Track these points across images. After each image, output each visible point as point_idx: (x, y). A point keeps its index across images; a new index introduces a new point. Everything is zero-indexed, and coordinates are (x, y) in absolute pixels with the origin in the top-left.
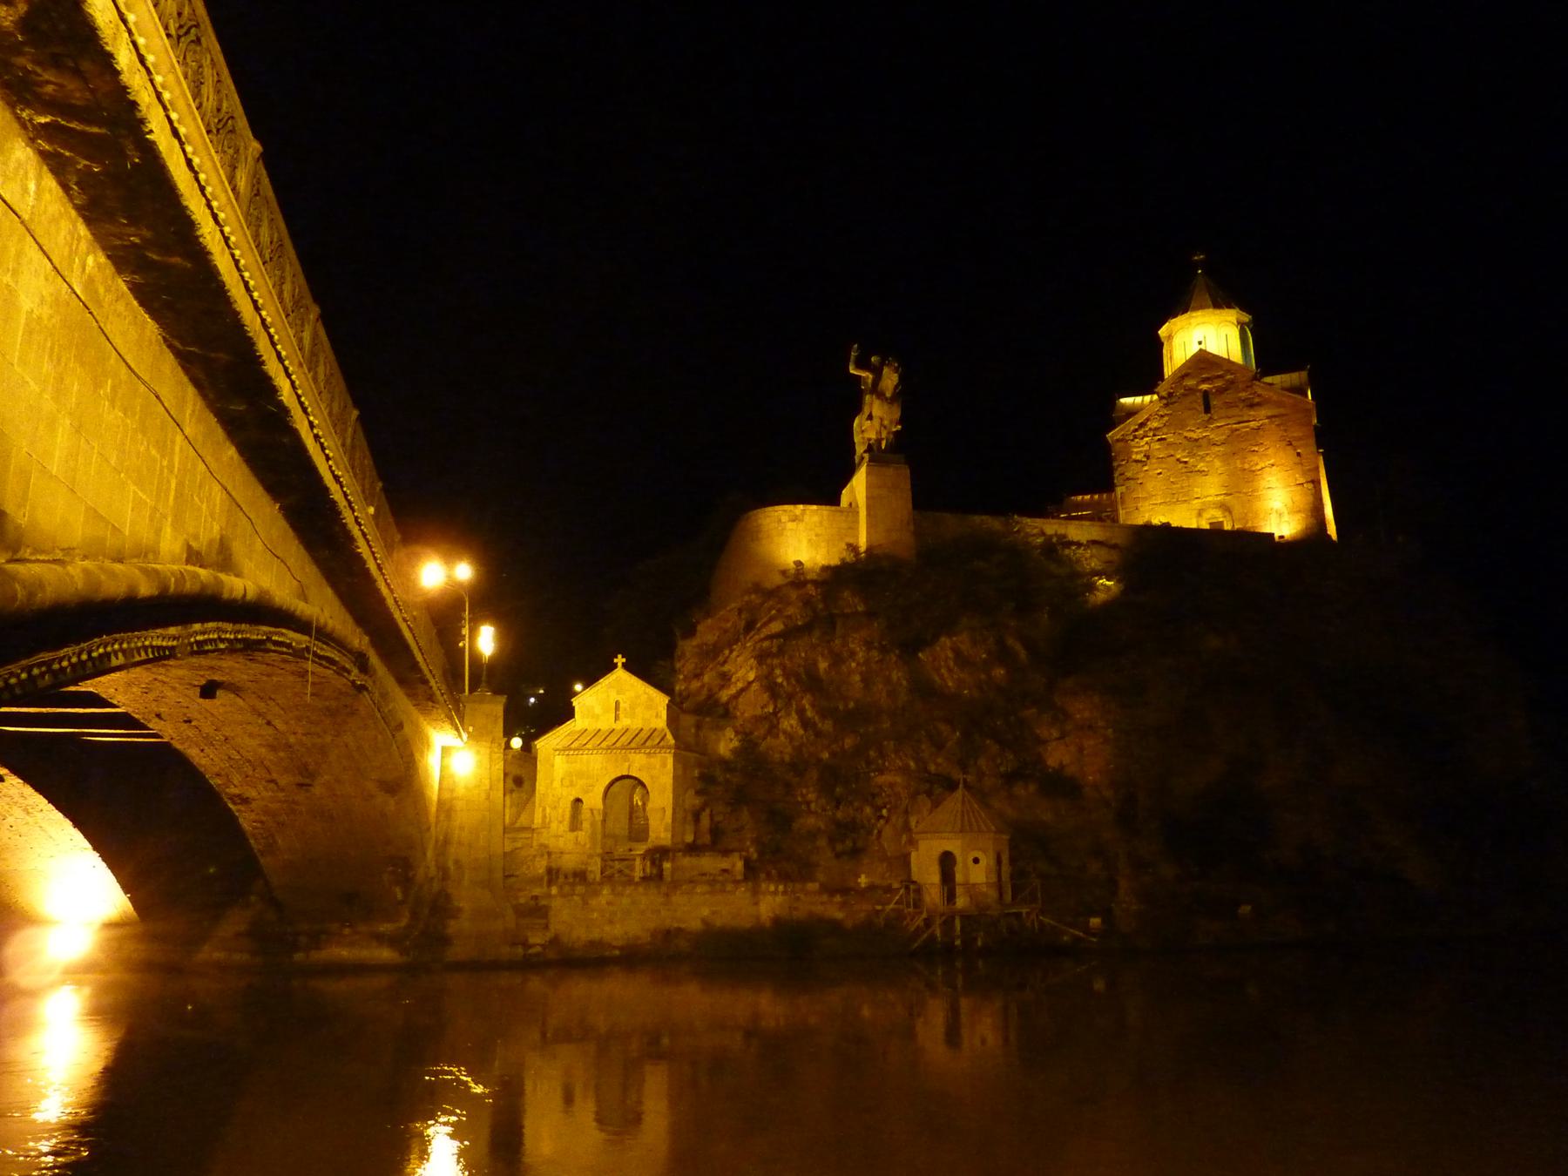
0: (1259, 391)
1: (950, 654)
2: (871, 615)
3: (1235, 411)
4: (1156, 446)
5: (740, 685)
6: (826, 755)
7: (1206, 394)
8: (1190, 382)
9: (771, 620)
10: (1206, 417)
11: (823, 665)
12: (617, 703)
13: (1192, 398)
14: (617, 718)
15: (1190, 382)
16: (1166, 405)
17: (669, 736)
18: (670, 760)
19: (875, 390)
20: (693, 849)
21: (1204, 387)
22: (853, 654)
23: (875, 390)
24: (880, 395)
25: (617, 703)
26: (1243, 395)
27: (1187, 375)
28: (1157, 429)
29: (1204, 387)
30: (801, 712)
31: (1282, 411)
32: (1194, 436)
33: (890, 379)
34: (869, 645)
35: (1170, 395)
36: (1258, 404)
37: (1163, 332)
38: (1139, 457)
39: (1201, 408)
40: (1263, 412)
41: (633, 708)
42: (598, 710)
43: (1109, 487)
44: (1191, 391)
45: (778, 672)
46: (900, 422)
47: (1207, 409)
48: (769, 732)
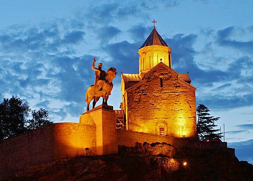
7: (161, 79)
8: (156, 74)
10: (161, 88)
16: (148, 81)
21: (161, 77)
28: (143, 90)
29: (161, 77)
32: (155, 94)
35: (149, 78)
36: (179, 86)
39: (160, 85)
40: (180, 90)
47: (162, 86)
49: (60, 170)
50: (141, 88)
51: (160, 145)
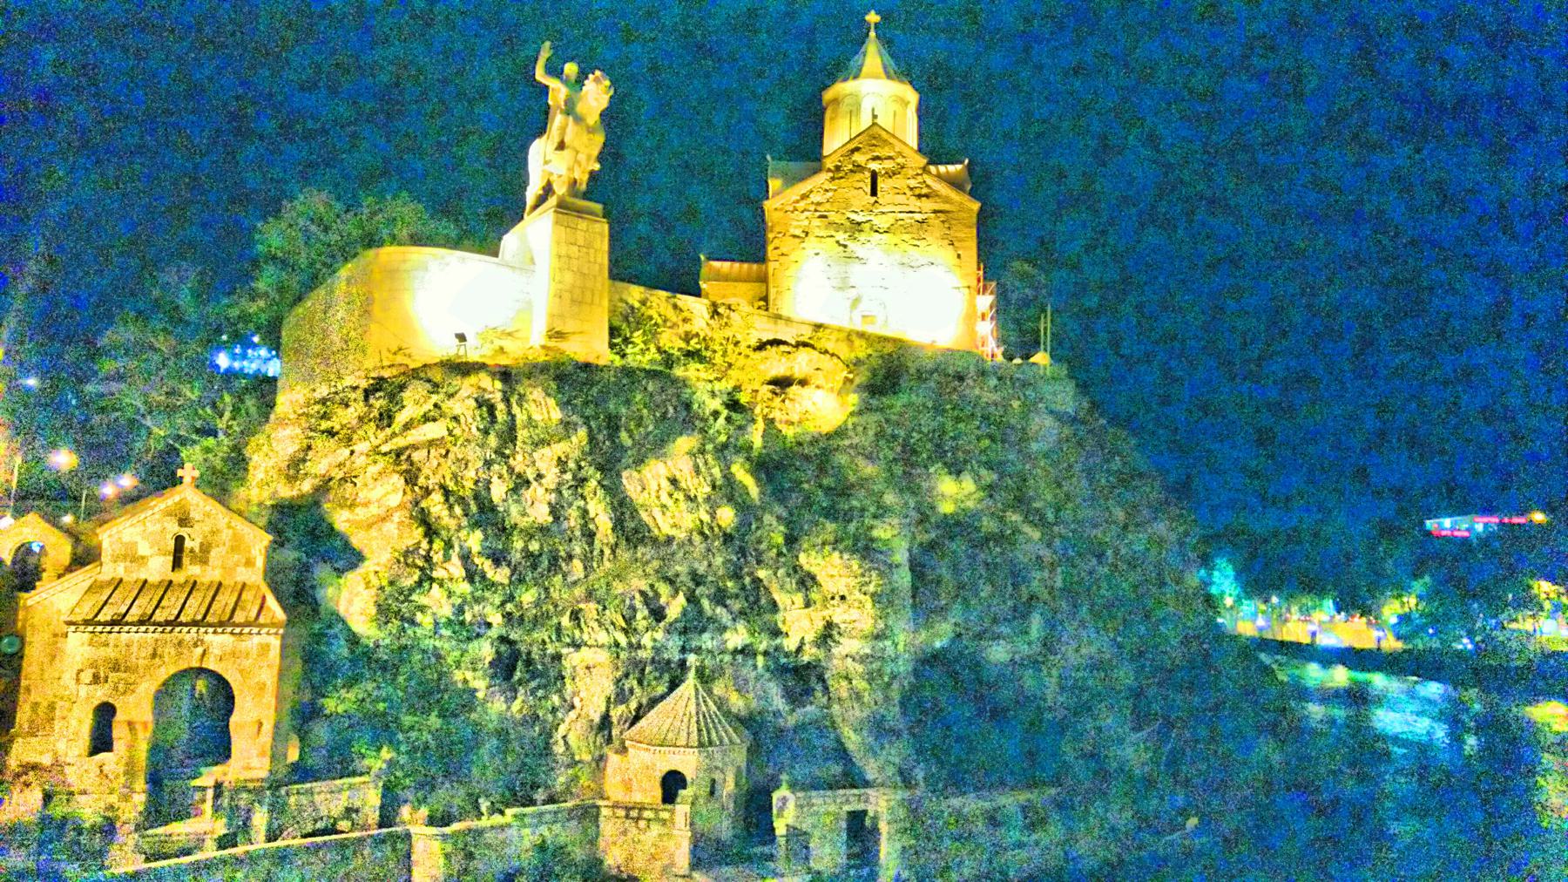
0: (929, 181)
1: (666, 485)
2: (568, 427)
3: (901, 199)
4: (818, 222)
5: (374, 510)
6: (496, 618)
9: (426, 419)
11: (498, 491)
12: (179, 541)
13: (858, 176)
14: (177, 564)
15: (857, 157)
16: (833, 179)
17: (272, 602)
18: (275, 642)
19: (570, 109)
20: (302, 773)
21: (874, 166)
22: (539, 476)
23: (570, 109)
24: (579, 120)
25: (179, 541)
26: (913, 183)
27: (857, 149)
28: (819, 204)
30: (466, 558)
31: (946, 207)
32: (858, 218)
33: (596, 95)
34: (562, 463)
35: (838, 168)
36: (927, 196)
37: (828, 95)
38: (798, 232)
39: (868, 189)
40: (928, 205)
41: (206, 549)
42: (143, 549)
43: (761, 258)
44: (858, 168)
45: (437, 497)
46: (600, 159)
47: (874, 193)
48: (420, 584)
49: (347, 406)
50: (815, 198)
51: (783, 348)
